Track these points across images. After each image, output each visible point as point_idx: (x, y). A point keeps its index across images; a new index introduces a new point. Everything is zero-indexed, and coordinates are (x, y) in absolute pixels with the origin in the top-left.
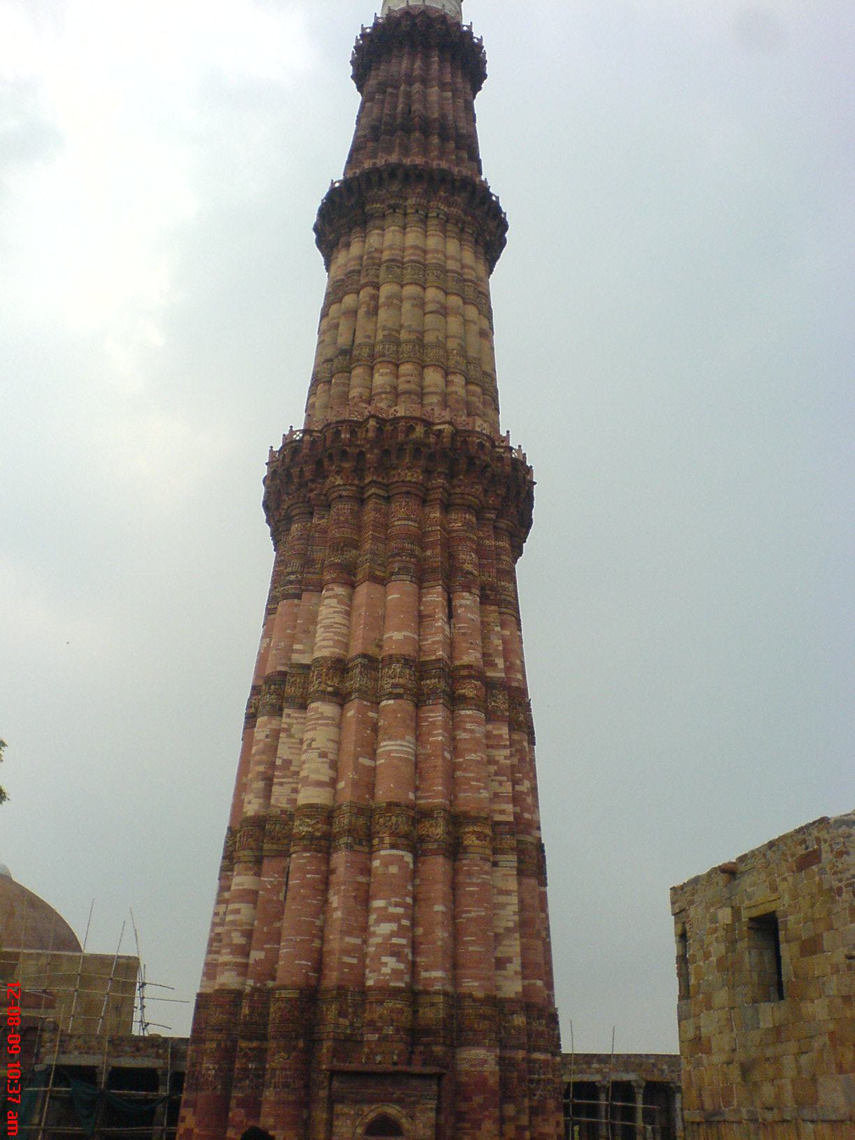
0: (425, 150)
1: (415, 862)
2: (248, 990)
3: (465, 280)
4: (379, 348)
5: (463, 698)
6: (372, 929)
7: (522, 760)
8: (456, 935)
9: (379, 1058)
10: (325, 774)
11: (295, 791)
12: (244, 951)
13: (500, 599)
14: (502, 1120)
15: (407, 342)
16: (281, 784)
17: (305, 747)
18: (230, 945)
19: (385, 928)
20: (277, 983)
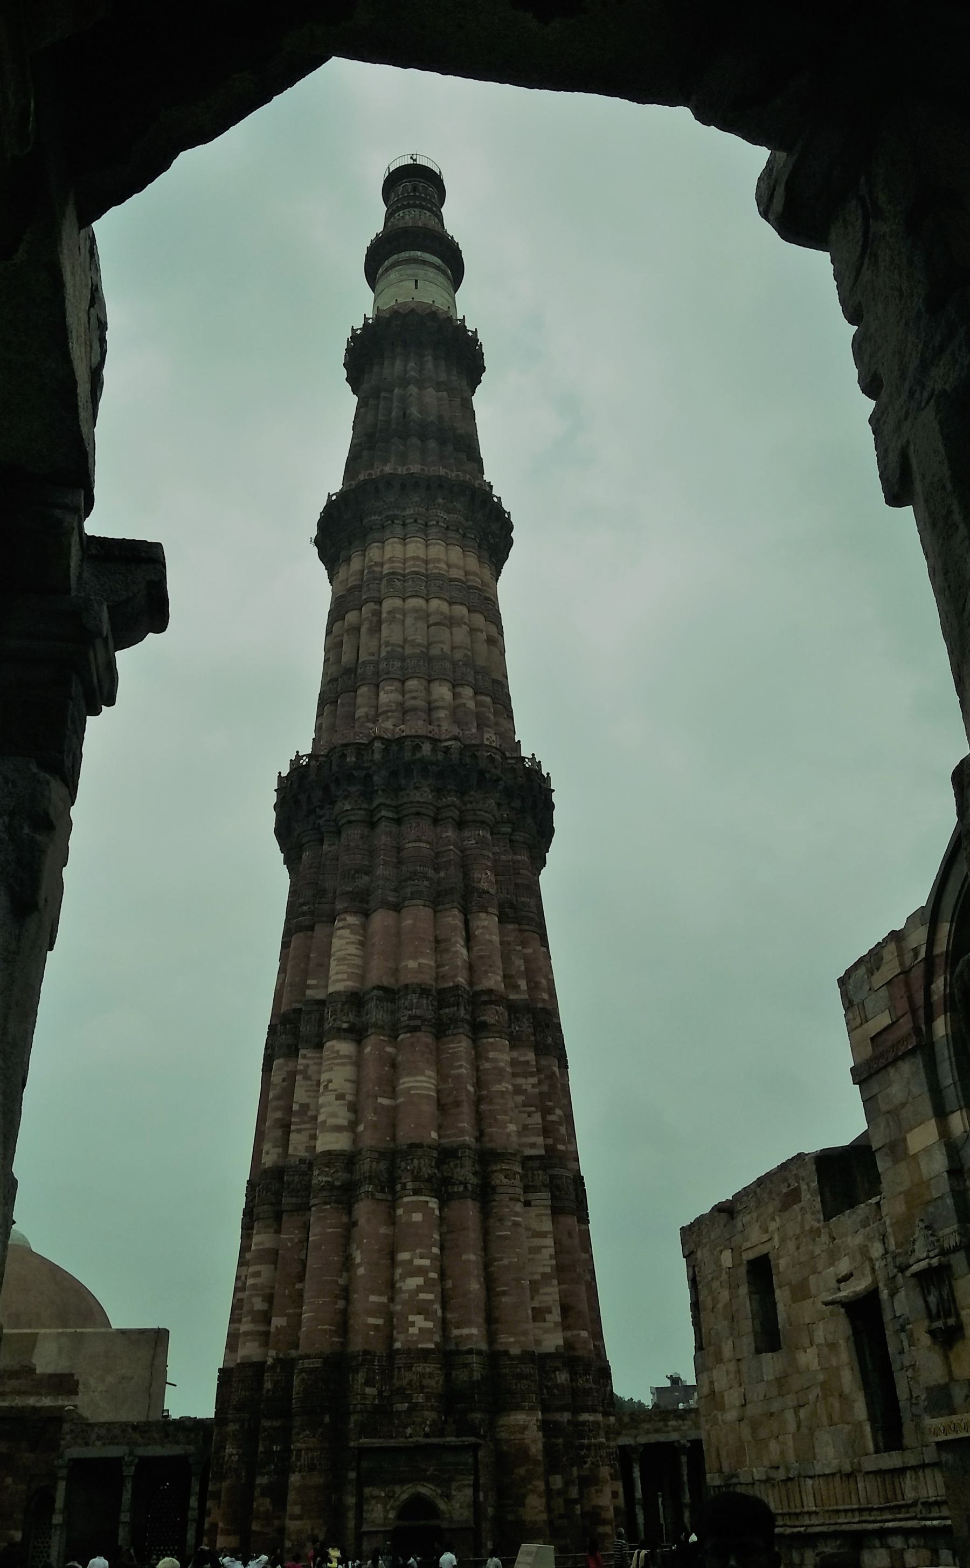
1: (441, 1209)
2: (270, 1361)
3: (470, 587)
4: (383, 666)
6: (398, 1285)
8: (489, 1282)
9: (409, 1431)
10: (343, 1117)
11: (314, 1137)
14: (549, 1493)
16: (299, 1131)
17: (321, 1090)
18: (251, 1312)
20: (301, 1351)
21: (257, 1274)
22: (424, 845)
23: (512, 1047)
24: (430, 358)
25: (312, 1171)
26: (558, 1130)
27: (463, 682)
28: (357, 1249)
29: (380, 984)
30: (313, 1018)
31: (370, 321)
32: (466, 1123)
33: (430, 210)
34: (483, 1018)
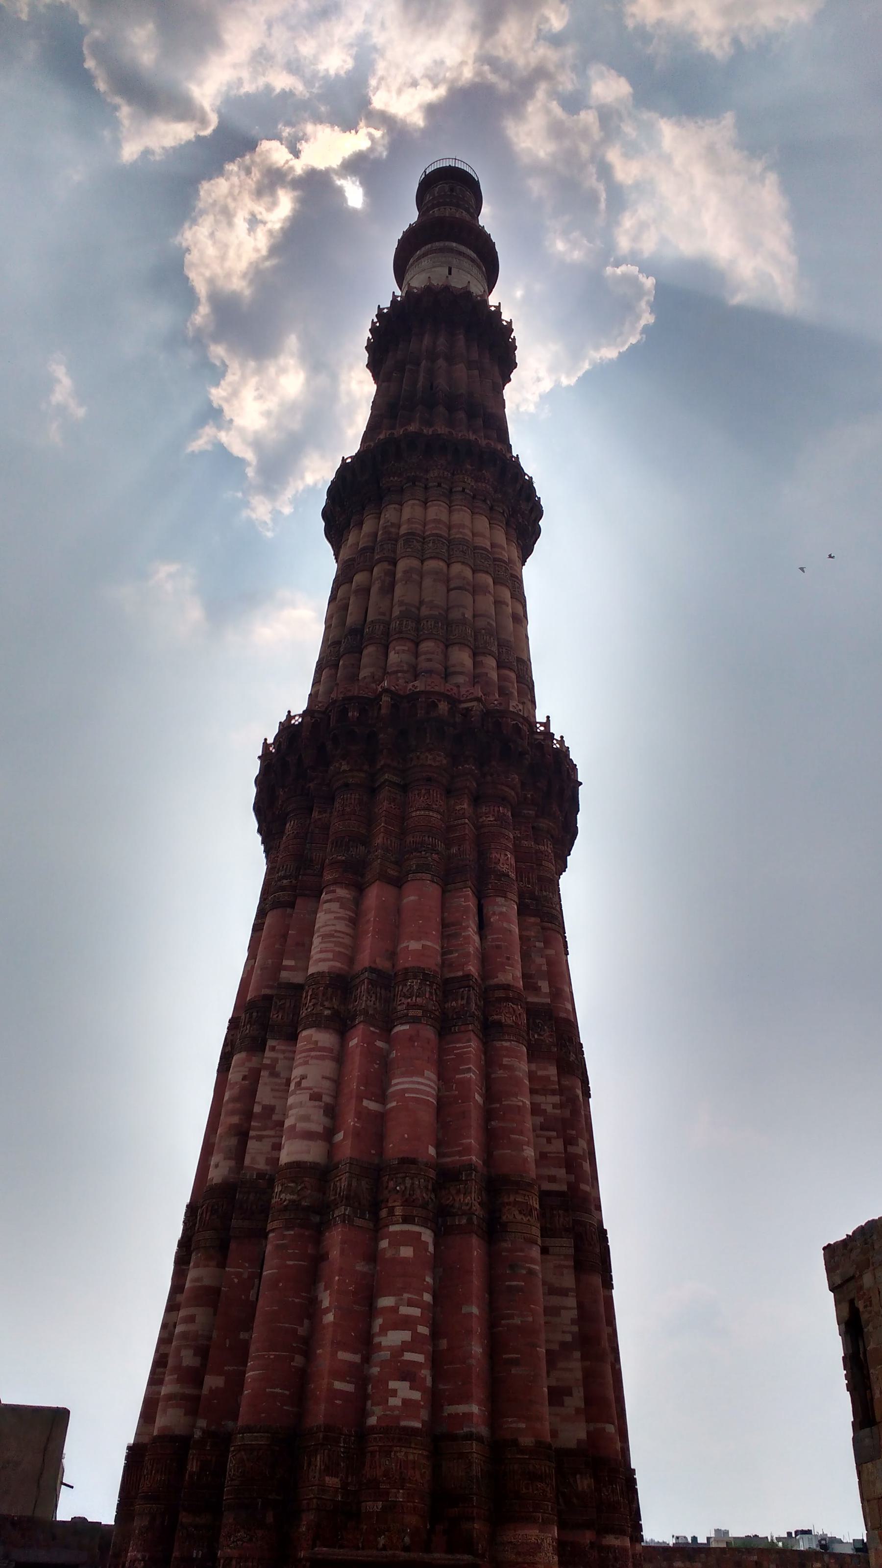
1: (436, 1245)
2: (198, 1434)
3: (495, 560)
4: (393, 625)
5: (499, 1024)
6: (377, 1340)
10: (317, 1122)
11: (278, 1147)
12: (195, 1377)
16: (259, 1138)
17: (292, 1087)
19: (396, 1338)
22: (435, 815)
23: (531, 1058)
24: (461, 336)
25: (273, 1188)
26: (581, 1166)
28: (325, 1290)
29: (373, 966)
30: (288, 1005)
31: (399, 299)
32: (473, 1140)
33: (467, 210)
34: (495, 1017)
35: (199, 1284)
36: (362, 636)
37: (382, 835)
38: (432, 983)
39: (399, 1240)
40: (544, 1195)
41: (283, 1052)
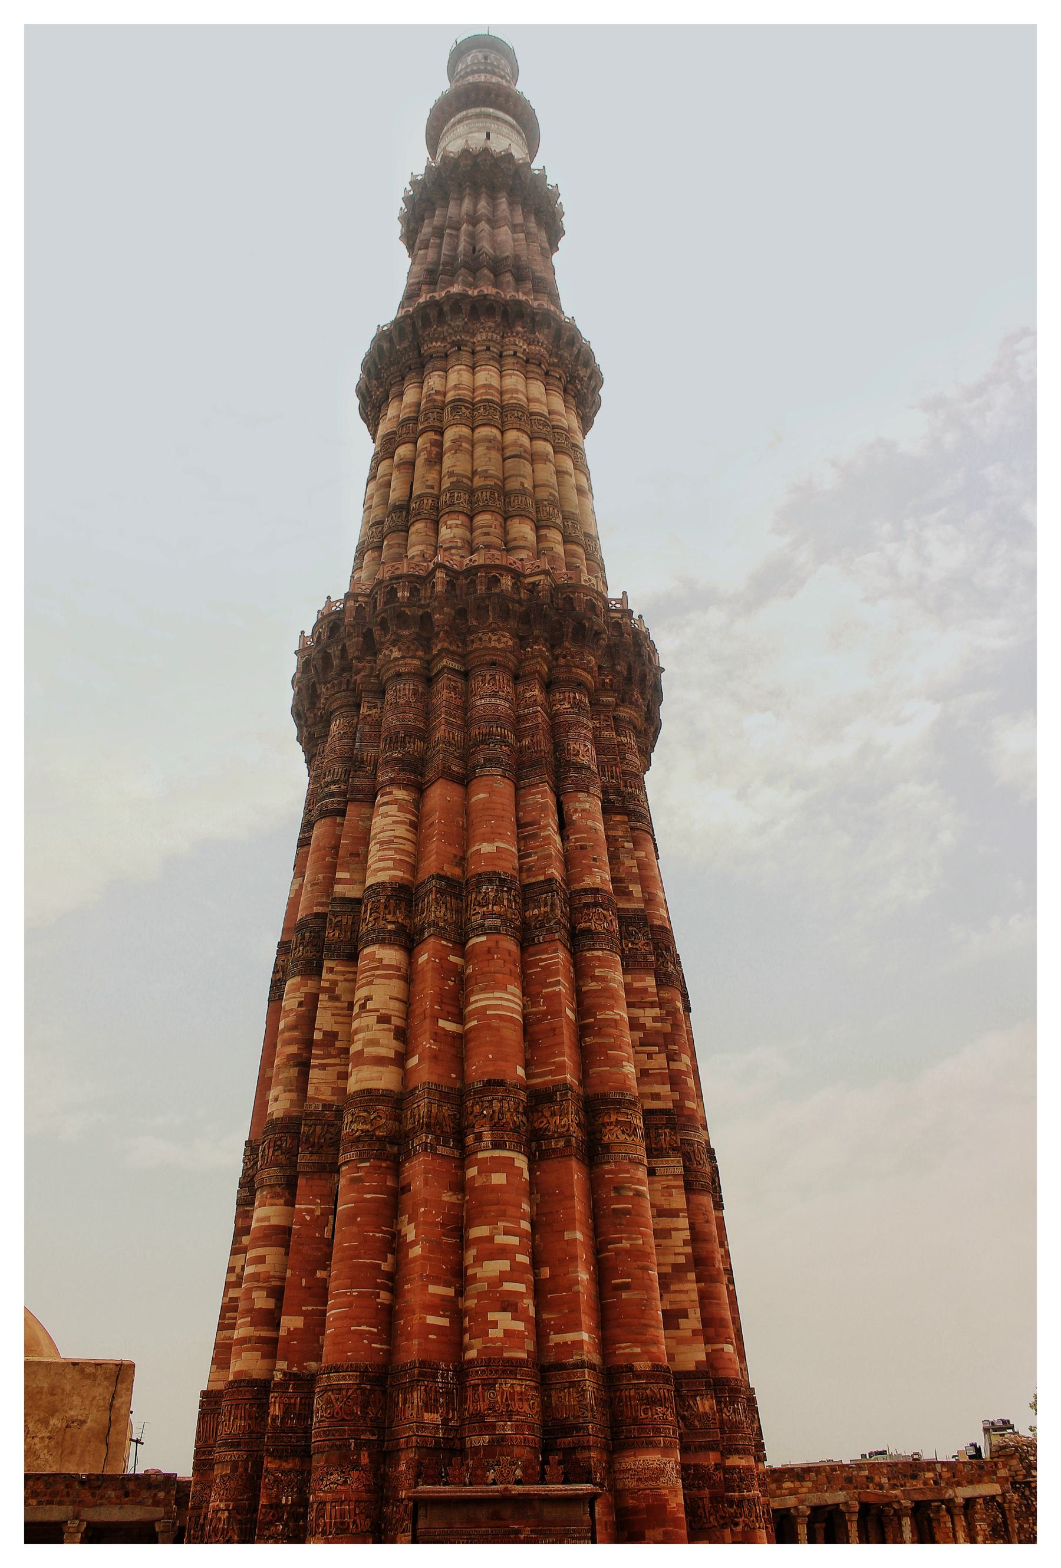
0: (496, 284)
1: (531, 1171)
2: (278, 1376)
3: (554, 427)
4: (443, 498)
5: (588, 931)
6: (470, 1272)
7: (676, 1026)
8: (602, 1272)
9: (491, 1475)
10: (388, 1047)
11: (344, 1076)
12: (271, 1319)
13: (627, 809)
15: (482, 488)
16: (323, 1067)
17: (356, 1009)
21: (261, 1260)
24: (504, 199)
27: (549, 523)
32: (567, 1058)
34: (583, 925)
35: (267, 1223)
36: (408, 513)
37: (442, 727)
38: (510, 889)
39: (488, 1168)
40: (648, 1113)
41: (343, 973)
